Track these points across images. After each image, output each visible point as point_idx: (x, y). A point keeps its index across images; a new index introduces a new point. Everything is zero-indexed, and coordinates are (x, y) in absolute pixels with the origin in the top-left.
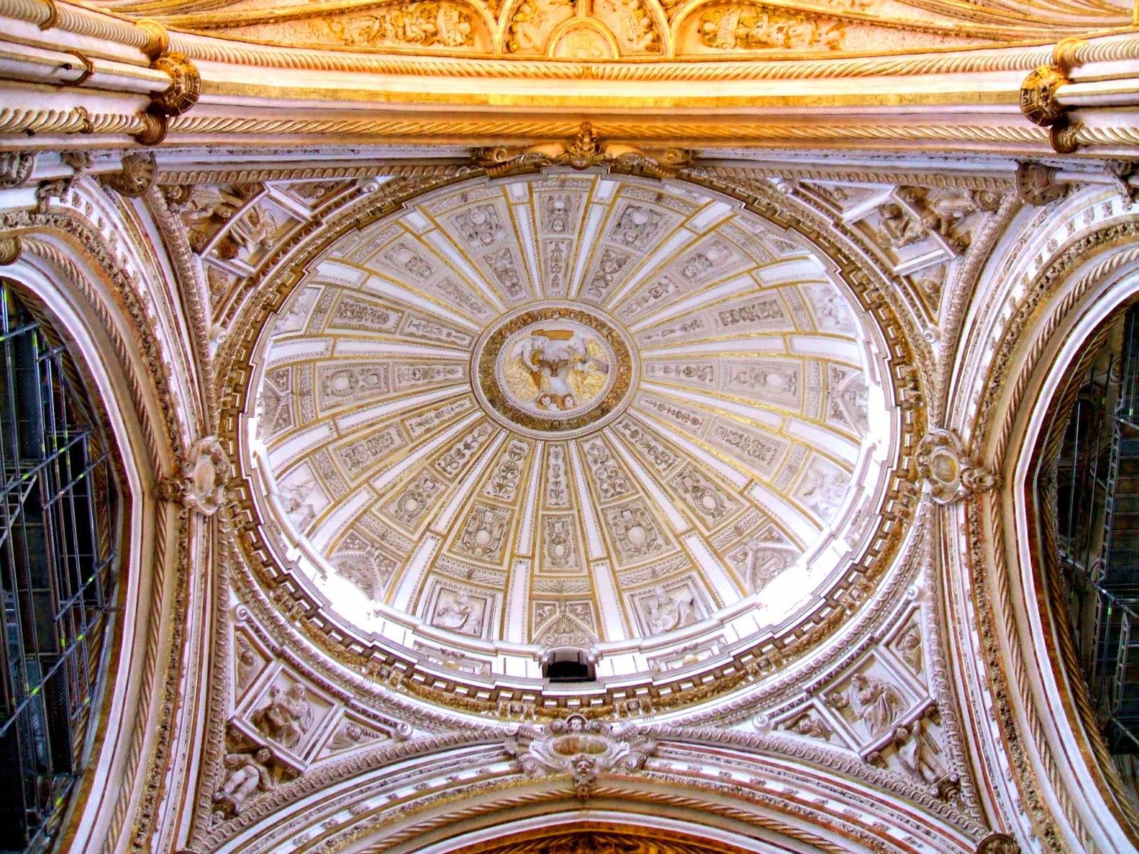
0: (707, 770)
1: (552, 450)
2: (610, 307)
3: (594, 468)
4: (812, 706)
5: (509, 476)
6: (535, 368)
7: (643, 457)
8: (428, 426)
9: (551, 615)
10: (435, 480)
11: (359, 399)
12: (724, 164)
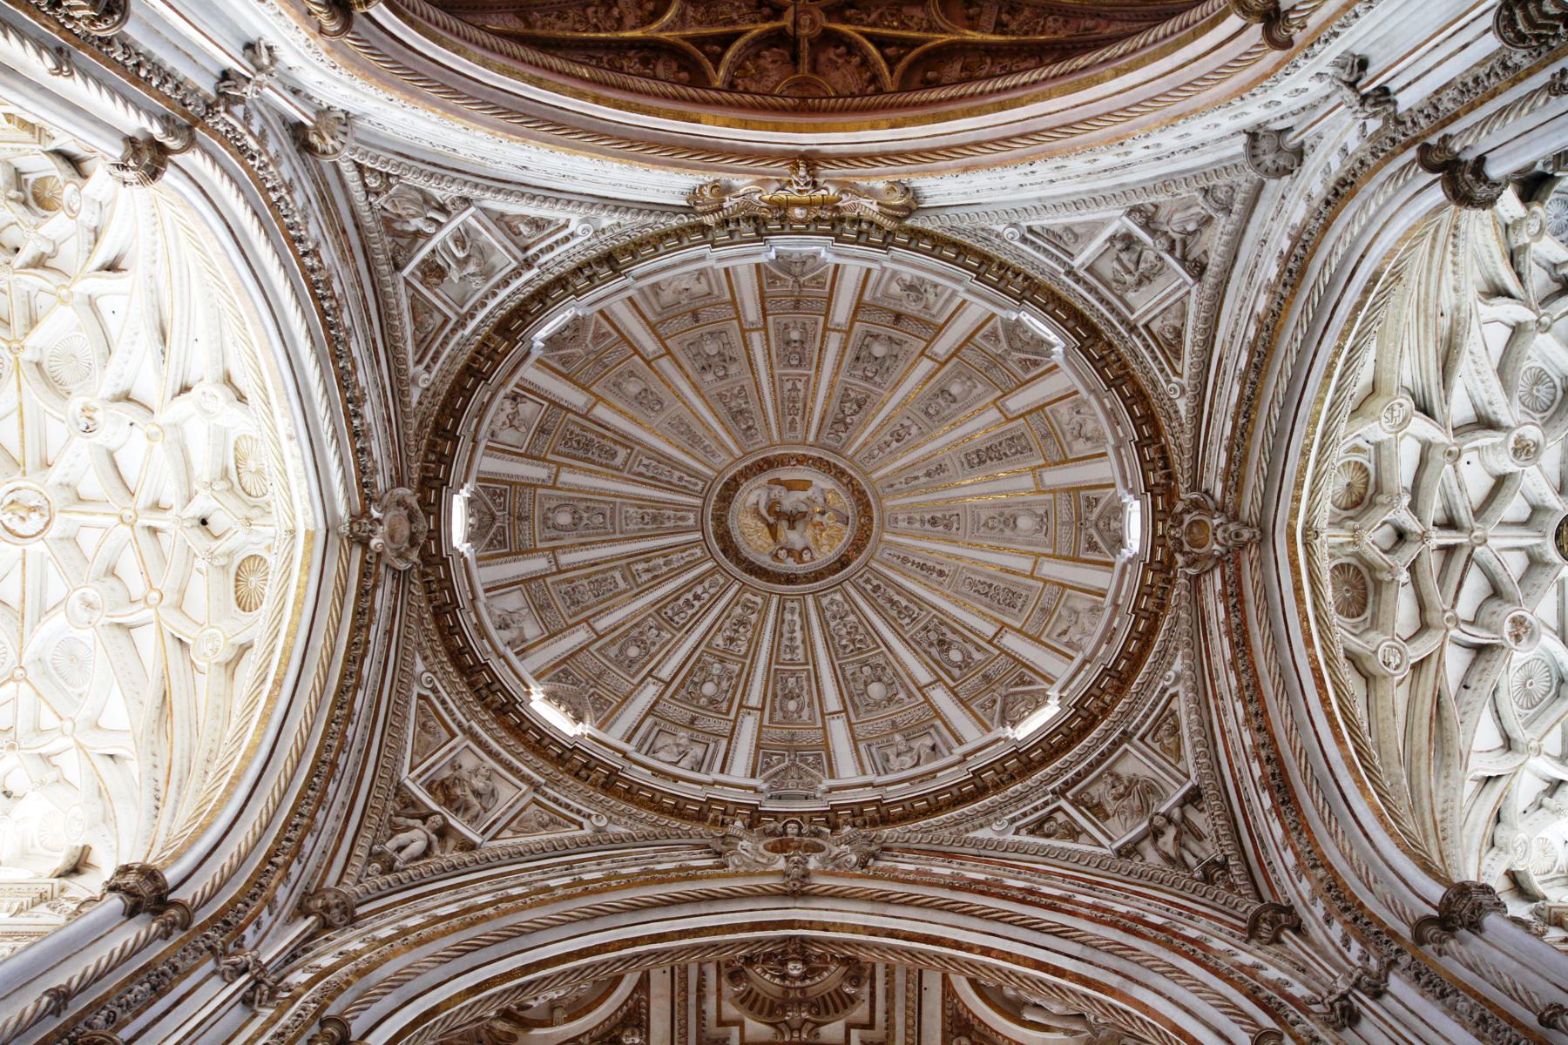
0: (936, 870)
1: (789, 605)
2: (850, 453)
3: (833, 624)
4: (1059, 809)
5: (742, 630)
6: (771, 520)
7: (885, 611)
10: (659, 629)
11: (582, 536)
12: (949, 212)
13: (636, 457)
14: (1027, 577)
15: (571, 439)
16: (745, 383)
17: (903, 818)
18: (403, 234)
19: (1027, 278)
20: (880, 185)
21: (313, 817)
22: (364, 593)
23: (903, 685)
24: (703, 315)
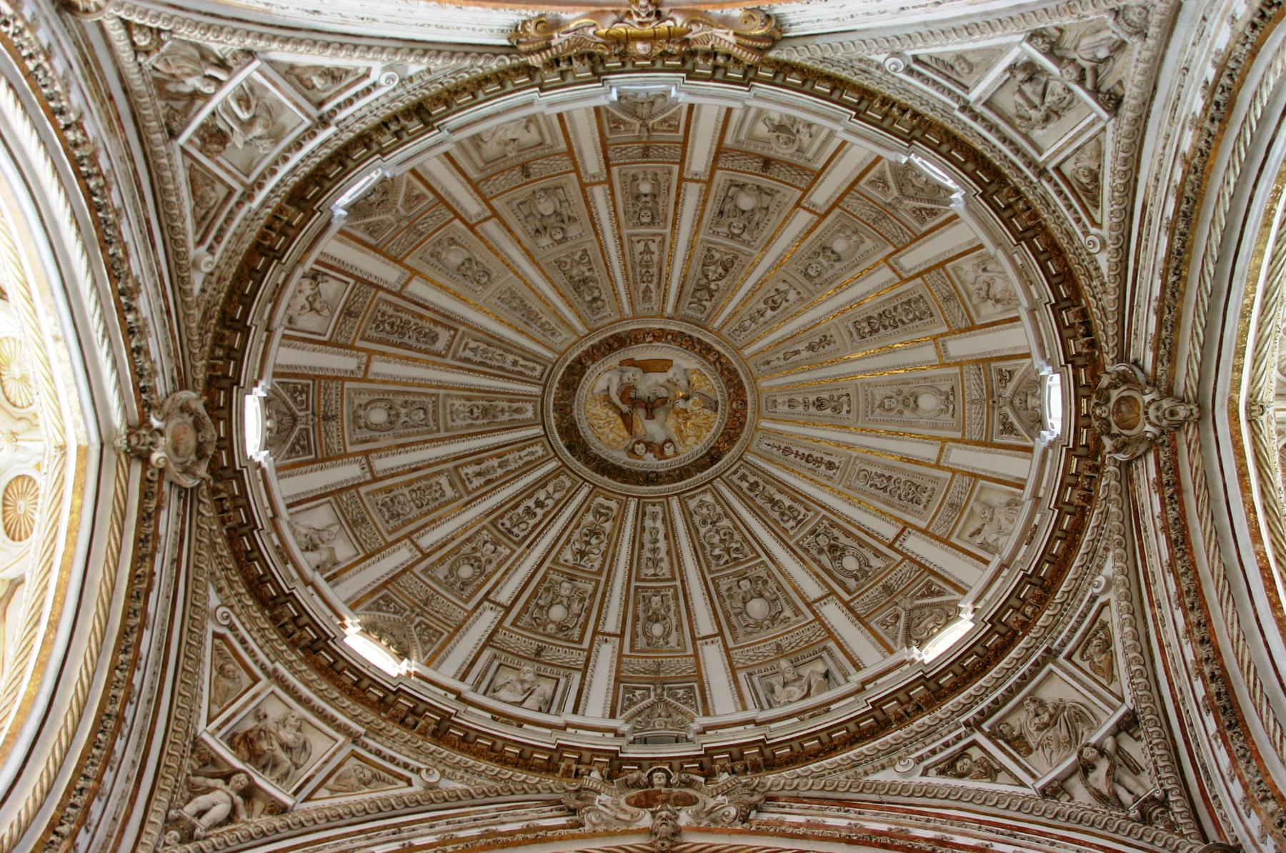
0: (830, 821)
1: (649, 509)
2: (716, 325)
3: (703, 530)
5: (594, 541)
6: (625, 408)
7: (765, 513)
8: (489, 477)
9: (643, 699)
10: (496, 543)
11: (400, 436)
12: (819, 40)
13: (461, 339)
14: (932, 466)
15: (383, 322)
16: (588, 246)
17: (791, 761)
18: (178, 96)
19: (916, 115)
20: (736, 13)
21: (99, 780)
22: (146, 517)
23: (789, 601)
24: (535, 168)
